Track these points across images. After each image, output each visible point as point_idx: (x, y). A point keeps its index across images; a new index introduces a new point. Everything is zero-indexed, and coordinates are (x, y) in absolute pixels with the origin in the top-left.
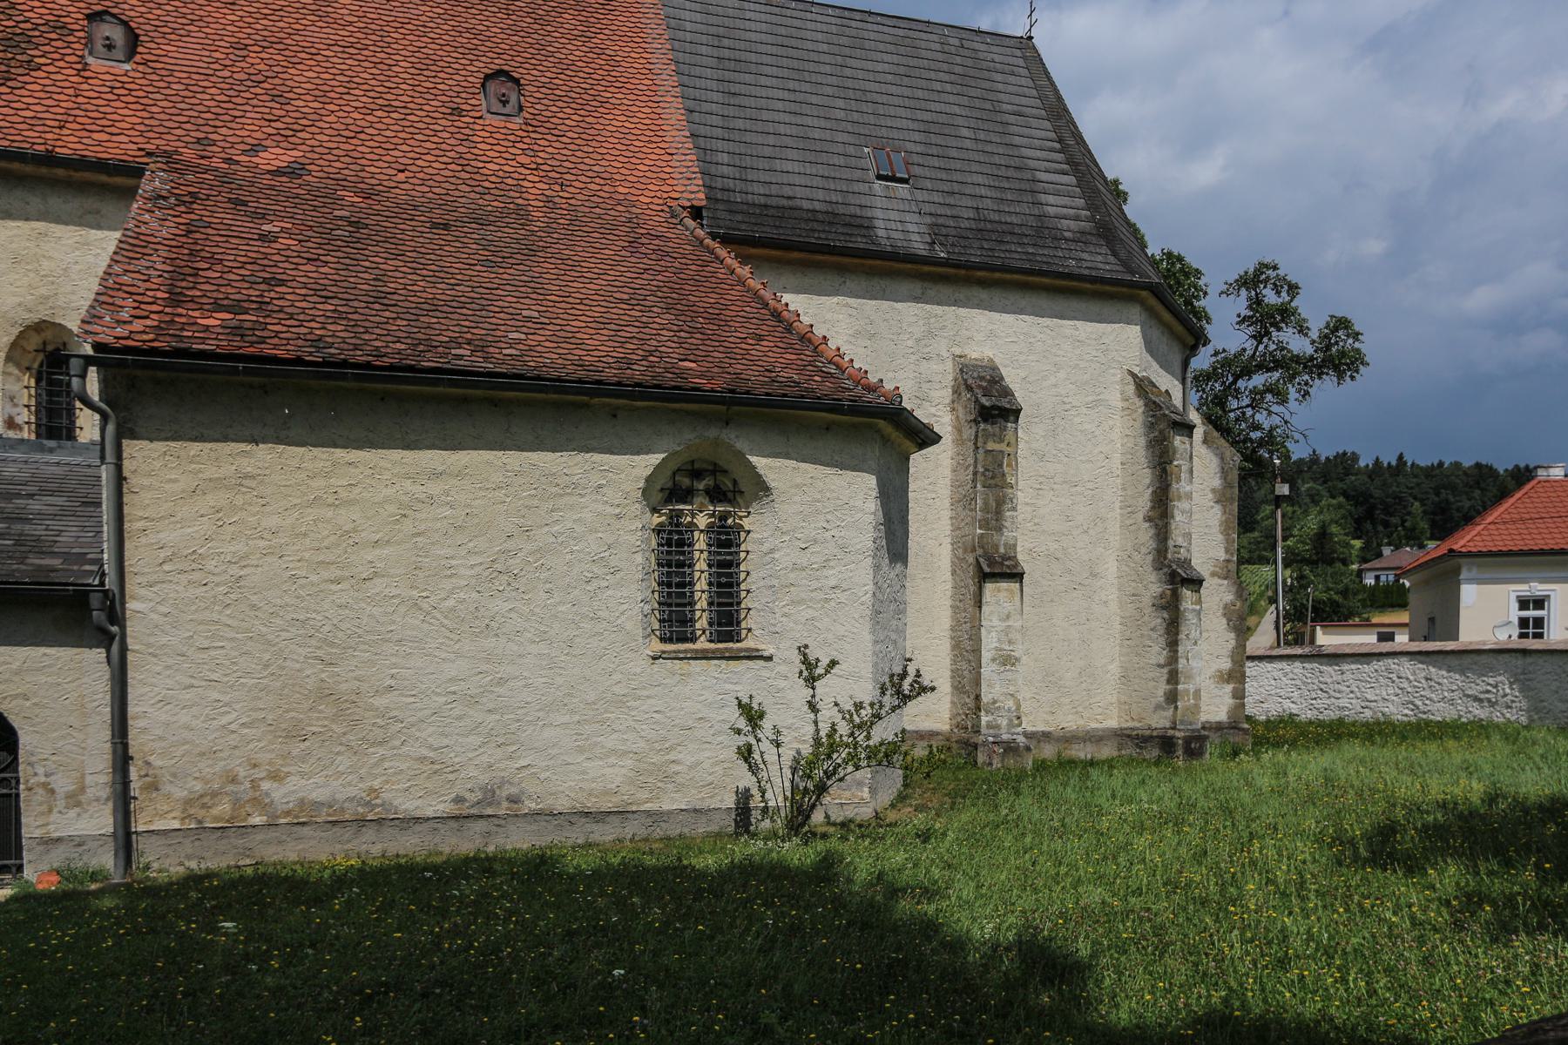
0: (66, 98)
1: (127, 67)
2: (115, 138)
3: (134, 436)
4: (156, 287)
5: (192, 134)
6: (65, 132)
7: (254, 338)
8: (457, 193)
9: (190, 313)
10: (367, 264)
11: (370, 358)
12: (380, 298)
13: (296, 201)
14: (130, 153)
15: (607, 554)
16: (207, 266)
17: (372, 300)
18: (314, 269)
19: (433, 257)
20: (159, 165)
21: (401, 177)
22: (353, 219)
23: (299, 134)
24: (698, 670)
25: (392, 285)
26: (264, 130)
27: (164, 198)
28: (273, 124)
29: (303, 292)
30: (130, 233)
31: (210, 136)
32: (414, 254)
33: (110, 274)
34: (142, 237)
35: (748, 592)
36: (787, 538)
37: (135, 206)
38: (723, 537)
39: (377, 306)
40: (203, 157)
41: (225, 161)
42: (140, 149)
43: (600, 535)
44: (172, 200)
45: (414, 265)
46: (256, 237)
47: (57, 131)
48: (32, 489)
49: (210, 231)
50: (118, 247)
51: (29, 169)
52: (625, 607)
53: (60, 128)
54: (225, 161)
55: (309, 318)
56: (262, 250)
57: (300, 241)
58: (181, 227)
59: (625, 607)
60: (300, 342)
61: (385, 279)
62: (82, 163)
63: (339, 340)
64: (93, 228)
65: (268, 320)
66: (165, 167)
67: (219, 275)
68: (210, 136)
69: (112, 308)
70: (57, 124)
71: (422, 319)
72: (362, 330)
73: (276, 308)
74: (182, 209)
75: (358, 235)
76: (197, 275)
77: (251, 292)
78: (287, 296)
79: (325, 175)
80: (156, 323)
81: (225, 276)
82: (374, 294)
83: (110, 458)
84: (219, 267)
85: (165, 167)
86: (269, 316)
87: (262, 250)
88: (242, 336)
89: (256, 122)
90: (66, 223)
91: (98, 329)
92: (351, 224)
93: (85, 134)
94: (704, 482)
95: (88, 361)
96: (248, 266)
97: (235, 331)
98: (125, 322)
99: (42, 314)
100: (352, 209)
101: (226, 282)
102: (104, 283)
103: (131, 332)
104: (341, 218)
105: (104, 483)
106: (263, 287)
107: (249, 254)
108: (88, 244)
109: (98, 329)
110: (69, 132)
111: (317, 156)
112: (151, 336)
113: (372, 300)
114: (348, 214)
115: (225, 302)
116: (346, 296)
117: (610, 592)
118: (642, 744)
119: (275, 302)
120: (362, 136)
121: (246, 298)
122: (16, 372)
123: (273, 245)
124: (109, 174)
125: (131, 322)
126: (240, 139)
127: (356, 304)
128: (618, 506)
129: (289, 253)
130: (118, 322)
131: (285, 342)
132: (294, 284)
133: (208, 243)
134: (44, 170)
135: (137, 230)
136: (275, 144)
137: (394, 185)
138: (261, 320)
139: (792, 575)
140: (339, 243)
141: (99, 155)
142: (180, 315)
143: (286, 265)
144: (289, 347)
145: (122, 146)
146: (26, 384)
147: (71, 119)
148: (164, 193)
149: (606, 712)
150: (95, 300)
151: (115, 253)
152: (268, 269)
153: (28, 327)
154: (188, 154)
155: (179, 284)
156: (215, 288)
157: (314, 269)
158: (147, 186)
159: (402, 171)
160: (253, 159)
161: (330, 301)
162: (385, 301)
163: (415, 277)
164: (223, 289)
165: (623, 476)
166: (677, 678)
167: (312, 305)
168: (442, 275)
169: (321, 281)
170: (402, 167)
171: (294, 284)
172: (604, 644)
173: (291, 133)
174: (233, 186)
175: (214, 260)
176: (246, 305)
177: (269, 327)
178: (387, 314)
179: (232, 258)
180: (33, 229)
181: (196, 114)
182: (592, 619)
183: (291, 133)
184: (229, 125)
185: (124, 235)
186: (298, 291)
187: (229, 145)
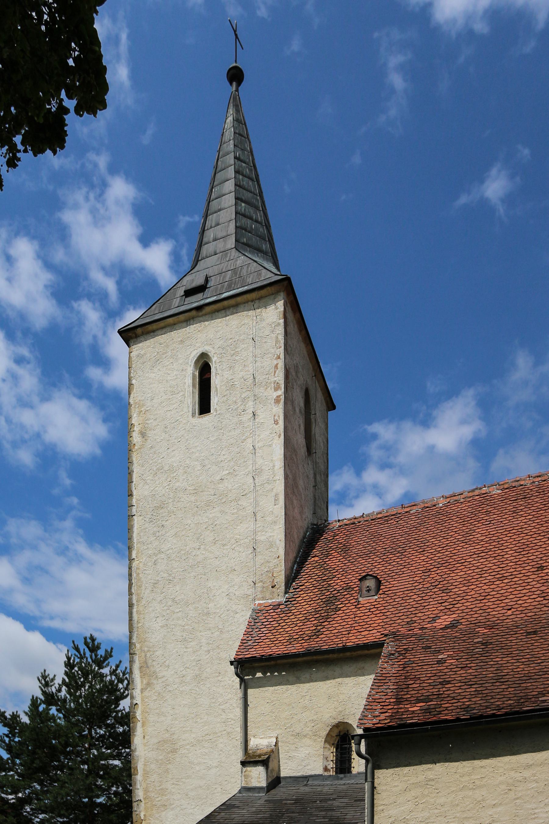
0: (351, 619)
1: (376, 597)
2: (371, 632)
3: (380, 768)
4: (390, 697)
5: (405, 620)
6: (351, 635)
7: (436, 713)
8: (541, 613)
9: (406, 706)
10: (492, 663)
11: (495, 711)
12: (499, 679)
13: (455, 639)
14: (377, 637)
16: (413, 682)
17: (495, 681)
18: (465, 672)
19: (528, 651)
20: (391, 639)
21: (510, 612)
22: (484, 642)
23: (456, 606)
25: (505, 671)
26: (438, 608)
27: (393, 654)
28: (443, 605)
29: (459, 684)
30: (378, 675)
31: (413, 619)
32: (518, 652)
33: (370, 695)
34: (384, 675)
37: (380, 661)
39: (498, 684)
40: (410, 630)
41: (421, 629)
42: (382, 634)
44: (397, 655)
45: (518, 657)
46: (436, 663)
47: (347, 636)
48: (334, 796)
49: (414, 665)
50: (373, 682)
51: (335, 656)
53: (348, 634)
54: (421, 629)
55: (462, 697)
56: (439, 668)
57: (457, 659)
58: (401, 666)
60: (458, 710)
61: (502, 668)
62: (358, 647)
63: (478, 705)
64: (361, 676)
65: (442, 702)
66: (393, 640)
67: (418, 685)
68: (413, 619)
69: (371, 711)
70: (347, 632)
71: (522, 685)
72: (490, 698)
73: (446, 696)
74: (401, 657)
75: (487, 649)
76: (408, 687)
77: (434, 690)
78: (452, 689)
79: (469, 623)
80: (390, 714)
81: (421, 685)
82: (496, 678)
83: (369, 779)
84: (418, 682)
85: (393, 640)
86: (442, 700)
87: (439, 668)
88: (430, 712)
89: (435, 606)
90: (350, 677)
91: (366, 721)
92: (483, 644)
93: (359, 634)
95: (361, 736)
96: (432, 678)
97: (426, 711)
98: (377, 716)
99: (340, 719)
100: (483, 636)
101: (422, 688)
102: (368, 700)
103: (380, 720)
104: (478, 643)
105: (366, 790)
106: (440, 686)
107: (433, 672)
108: (359, 684)
109: (366, 721)
110: (352, 635)
111: (465, 614)
112: (389, 721)
113: (495, 681)
114: (481, 640)
115: (422, 698)
116: (481, 682)
119: (445, 693)
120: (488, 597)
121: (431, 694)
122: (329, 746)
123: (444, 665)
124: (368, 650)
125: (379, 716)
126: (427, 617)
127: (487, 685)
129: (452, 667)
130: (374, 716)
131: (450, 712)
132: (455, 682)
133: (413, 671)
134: (341, 655)
135: (381, 672)
136: (444, 614)
137: (505, 618)
138: (439, 703)
140: (477, 656)
141: (365, 642)
142: (401, 708)
143: (451, 673)
144: (453, 714)
145: (374, 635)
146: (332, 751)
147: (353, 628)
148: (393, 652)
150: (364, 709)
151: (372, 685)
152: (442, 677)
153: (334, 726)
154: (403, 630)
155: (400, 693)
156: (417, 692)
157: (465, 672)
158: (386, 650)
159: (510, 609)
160: (433, 625)
161: (473, 686)
162: (502, 680)
163: (518, 664)
164: (420, 692)
167: (463, 691)
168: (533, 659)
169: (468, 677)
170: (510, 607)
171: (455, 682)
173: (452, 606)
174: (424, 640)
175: (416, 679)
176: (431, 697)
177: (443, 706)
178: (503, 687)
179: (424, 675)
180: (337, 682)
181: (407, 610)
183: (452, 606)
184: (422, 611)
185: (376, 676)
186: (457, 685)
187: (422, 621)
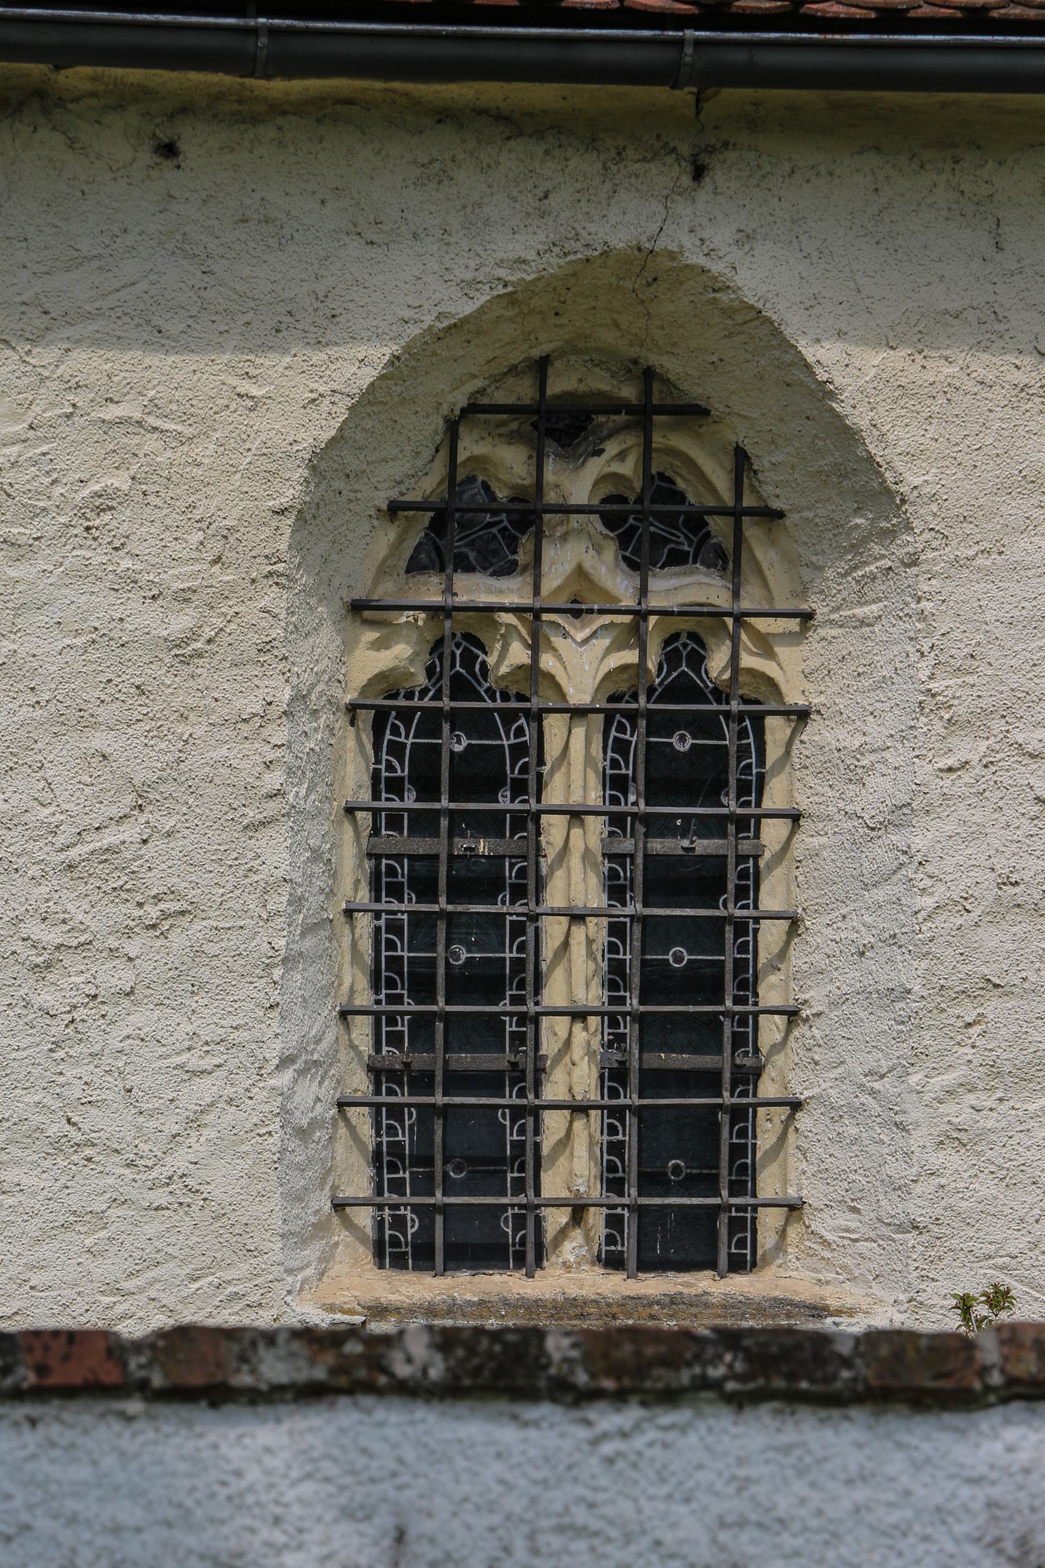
94: (595, 467)
128: (184, 597)
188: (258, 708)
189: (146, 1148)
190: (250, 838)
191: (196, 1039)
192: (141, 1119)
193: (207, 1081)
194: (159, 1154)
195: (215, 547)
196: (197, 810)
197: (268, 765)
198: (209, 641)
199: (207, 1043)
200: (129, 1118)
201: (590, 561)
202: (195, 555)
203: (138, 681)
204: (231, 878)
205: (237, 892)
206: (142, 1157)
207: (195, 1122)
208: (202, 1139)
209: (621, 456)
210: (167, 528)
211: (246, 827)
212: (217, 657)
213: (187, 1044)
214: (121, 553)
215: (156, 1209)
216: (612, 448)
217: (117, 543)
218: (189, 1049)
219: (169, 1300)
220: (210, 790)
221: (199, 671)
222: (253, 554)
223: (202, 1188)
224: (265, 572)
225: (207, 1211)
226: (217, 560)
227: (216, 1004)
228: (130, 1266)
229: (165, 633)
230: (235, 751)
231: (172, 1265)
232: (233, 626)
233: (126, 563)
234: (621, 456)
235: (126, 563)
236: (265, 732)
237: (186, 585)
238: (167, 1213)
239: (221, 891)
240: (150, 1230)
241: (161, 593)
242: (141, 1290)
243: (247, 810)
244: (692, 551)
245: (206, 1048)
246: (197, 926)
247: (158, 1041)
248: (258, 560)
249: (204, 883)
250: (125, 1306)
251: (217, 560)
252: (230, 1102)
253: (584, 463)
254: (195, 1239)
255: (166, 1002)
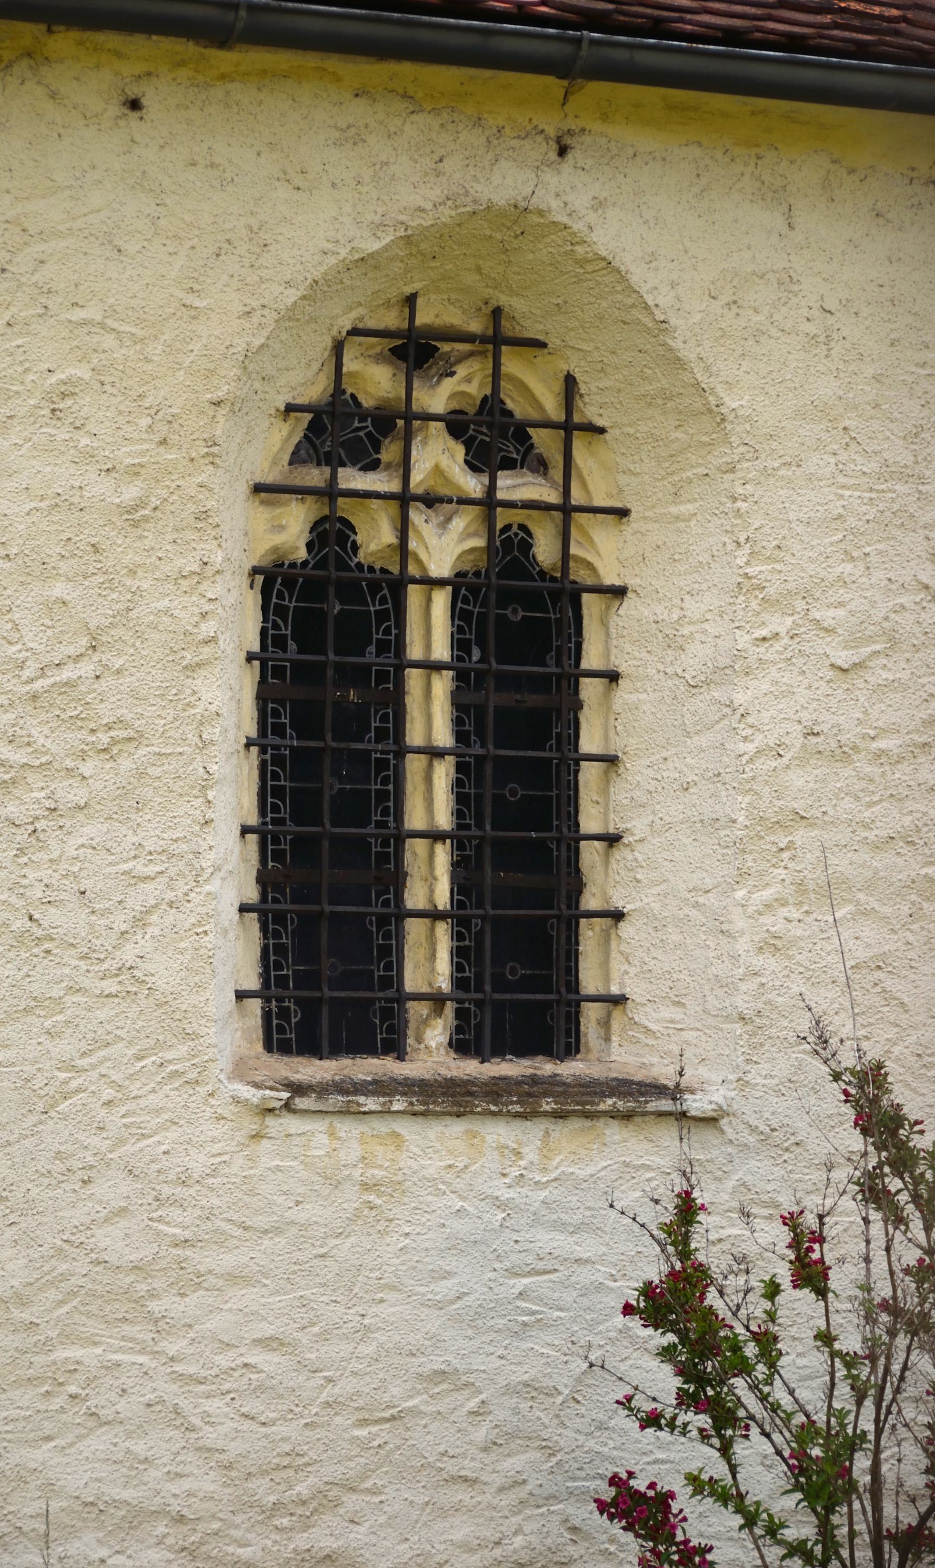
15: (86, 668)
24: (433, 1166)
35: (612, 840)
36: (780, 623)
38: (517, 615)
43: (59, 589)
52: (150, 892)
59: (150, 892)
94: (448, 386)
117: (93, 830)
118: (208, 1483)
128: (135, 471)
139: (798, 780)
149: (68, 1337)
165: (155, 350)
166: (351, 1198)
172: (64, 1048)
182: (20, 938)
188: (195, 567)
189: (98, 943)
190: (188, 677)
191: (141, 849)
192: (94, 918)
193: (149, 886)
194: (110, 948)
195: (163, 430)
196: (143, 652)
197: (204, 615)
198: (155, 509)
199: (150, 853)
200: (84, 917)
201: (445, 462)
202: (144, 436)
203: (94, 540)
204: (172, 712)
205: (177, 723)
206: (94, 951)
207: (140, 921)
208: (147, 937)
209: (468, 380)
210: (120, 413)
211: (186, 668)
212: (161, 523)
213: (133, 853)
214: (81, 432)
215: (107, 996)
216: (462, 371)
217: (78, 424)
218: (135, 857)
219: (116, 1076)
220: (155, 636)
221: (146, 534)
222: (192, 437)
223: (147, 979)
224: (202, 453)
225: (151, 999)
226: (164, 442)
227: (158, 819)
228: (83, 1046)
229: (118, 500)
230: (176, 603)
231: (121, 1045)
232: (175, 497)
233: (85, 441)
234: (468, 380)
235: (85, 441)
236: (201, 588)
237: (136, 461)
238: (116, 1000)
239: (163, 722)
240: (102, 1014)
241: (114, 468)
242: (93, 1067)
243: (185, 653)
244: (519, 458)
245: (149, 857)
246: (142, 751)
247: (108, 850)
248: (197, 443)
249: (149, 714)
250: (80, 1081)
251: (164, 442)
252: (171, 904)
253: (439, 382)
254: (141, 1023)
255: (115, 816)
